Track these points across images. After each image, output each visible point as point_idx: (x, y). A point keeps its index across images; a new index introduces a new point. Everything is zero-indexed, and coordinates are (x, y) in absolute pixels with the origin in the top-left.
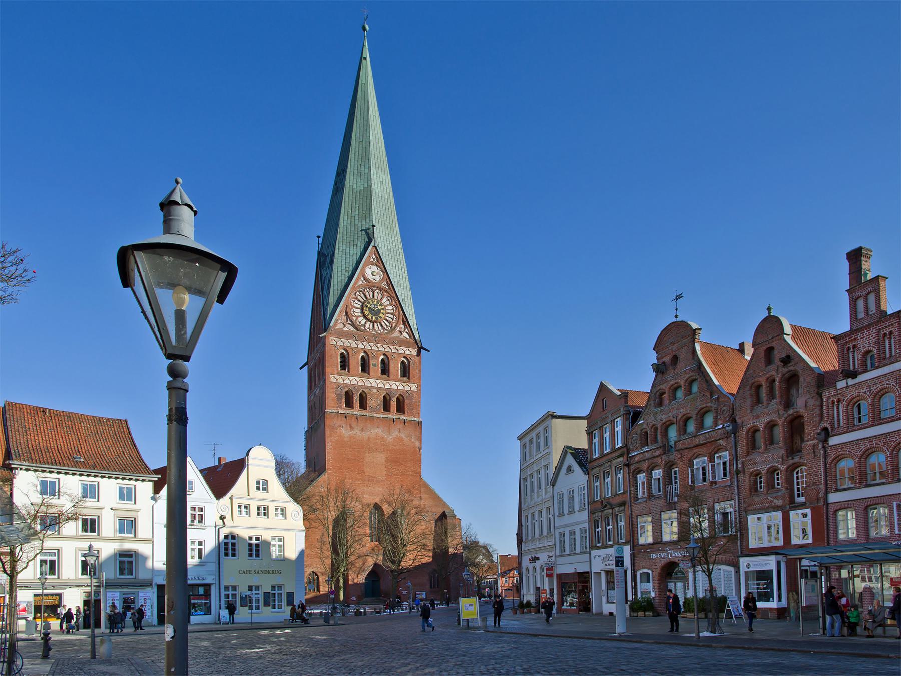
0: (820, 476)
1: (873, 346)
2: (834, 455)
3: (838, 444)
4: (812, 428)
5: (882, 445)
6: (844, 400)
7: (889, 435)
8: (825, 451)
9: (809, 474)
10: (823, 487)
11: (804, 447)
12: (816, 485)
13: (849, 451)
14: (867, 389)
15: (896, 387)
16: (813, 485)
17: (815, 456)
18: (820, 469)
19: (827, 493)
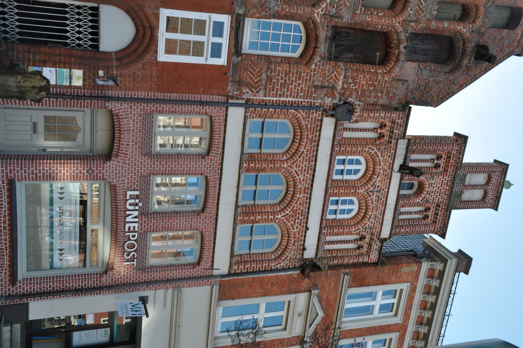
0: (279, 92)
1: (425, 196)
2: (306, 125)
3: (320, 135)
4: (362, 87)
5: (294, 206)
6: (379, 150)
7: (304, 218)
8: (317, 108)
9: (290, 71)
10: (260, 97)
11: (339, 67)
12: (266, 83)
13: (303, 152)
14: (378, 186)
15: (362, 228)
16: (267, 77)
17: (316, 87)
18: (291, 96)
19: (248, 105)
